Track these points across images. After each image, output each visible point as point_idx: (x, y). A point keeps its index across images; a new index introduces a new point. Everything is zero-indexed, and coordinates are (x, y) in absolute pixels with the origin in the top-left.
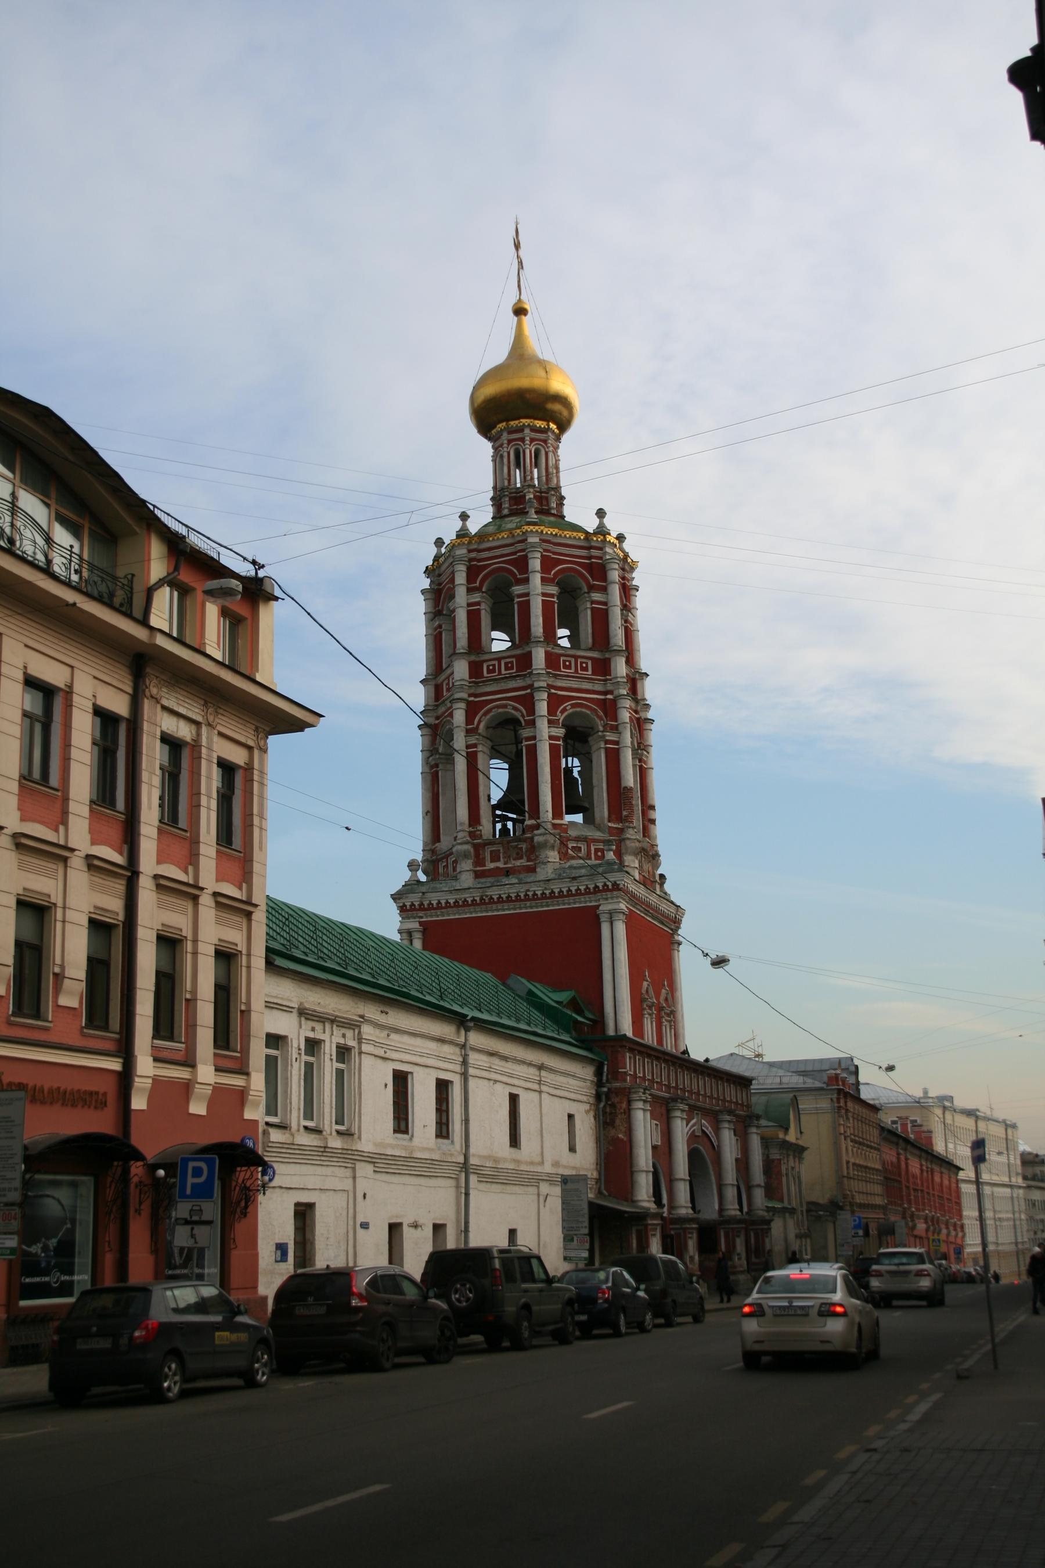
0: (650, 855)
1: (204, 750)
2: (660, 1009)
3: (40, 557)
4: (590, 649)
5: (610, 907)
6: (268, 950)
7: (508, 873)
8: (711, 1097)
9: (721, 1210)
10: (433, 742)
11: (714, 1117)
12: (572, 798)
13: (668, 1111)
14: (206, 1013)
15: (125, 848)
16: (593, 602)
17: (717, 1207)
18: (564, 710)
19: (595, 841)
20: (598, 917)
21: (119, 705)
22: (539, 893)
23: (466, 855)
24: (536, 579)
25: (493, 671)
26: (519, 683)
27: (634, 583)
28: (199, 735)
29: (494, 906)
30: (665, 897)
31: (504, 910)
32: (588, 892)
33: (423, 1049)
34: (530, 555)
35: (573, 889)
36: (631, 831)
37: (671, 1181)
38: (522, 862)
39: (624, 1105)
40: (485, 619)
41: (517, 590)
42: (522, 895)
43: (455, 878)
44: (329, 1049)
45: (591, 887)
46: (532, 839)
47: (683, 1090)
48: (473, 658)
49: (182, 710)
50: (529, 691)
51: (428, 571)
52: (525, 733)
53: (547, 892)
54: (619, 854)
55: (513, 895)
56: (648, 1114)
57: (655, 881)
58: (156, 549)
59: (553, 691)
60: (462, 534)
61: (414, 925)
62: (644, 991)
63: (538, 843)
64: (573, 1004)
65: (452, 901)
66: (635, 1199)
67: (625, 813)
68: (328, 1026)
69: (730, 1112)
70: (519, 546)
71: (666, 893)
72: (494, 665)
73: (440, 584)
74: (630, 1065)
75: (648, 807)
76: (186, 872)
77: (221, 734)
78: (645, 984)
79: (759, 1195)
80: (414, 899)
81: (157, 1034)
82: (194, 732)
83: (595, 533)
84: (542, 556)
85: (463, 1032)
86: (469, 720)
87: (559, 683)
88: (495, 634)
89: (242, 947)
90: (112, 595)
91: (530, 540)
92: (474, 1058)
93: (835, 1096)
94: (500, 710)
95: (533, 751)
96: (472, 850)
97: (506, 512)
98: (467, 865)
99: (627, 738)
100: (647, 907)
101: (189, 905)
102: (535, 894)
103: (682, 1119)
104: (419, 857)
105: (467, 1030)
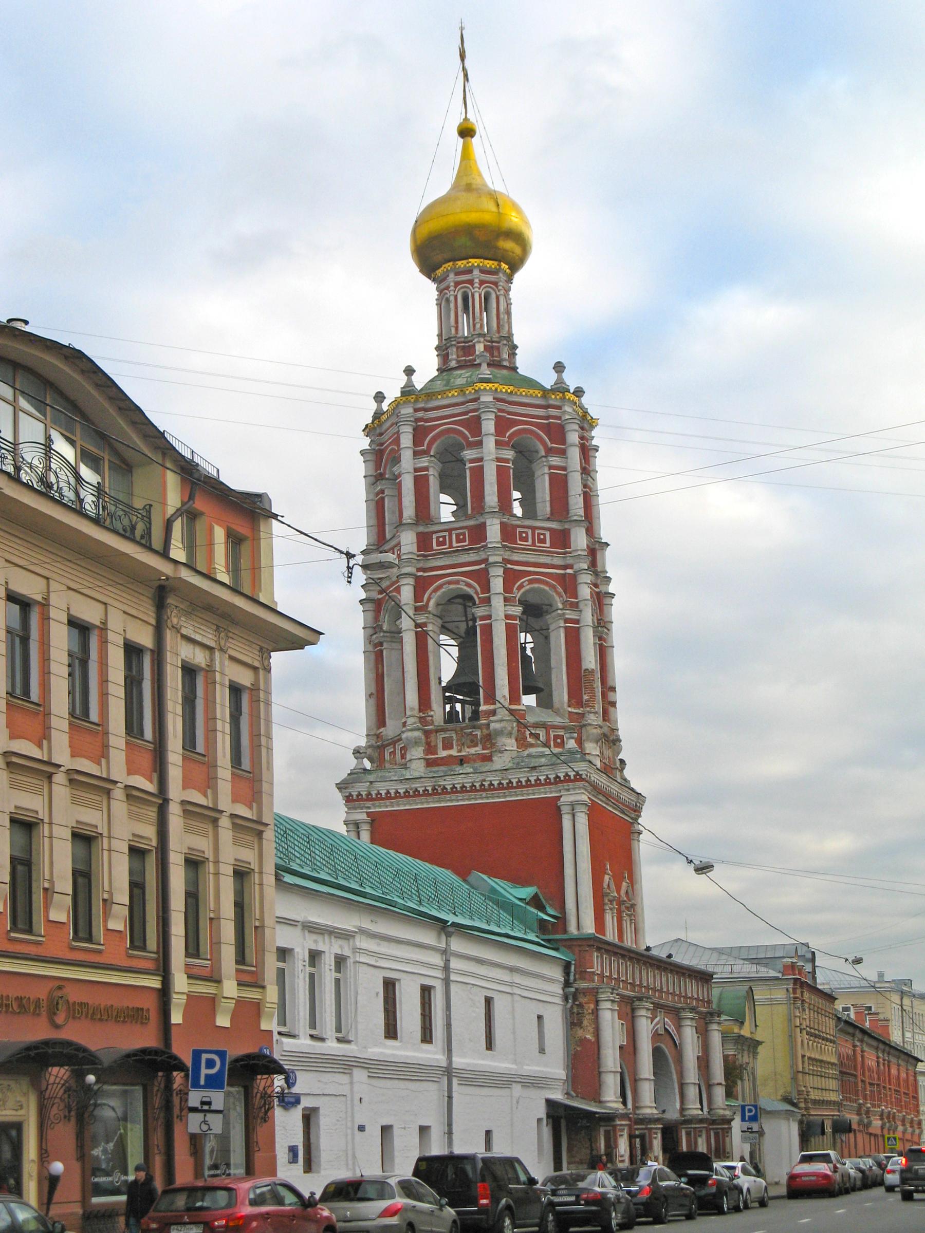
0: (611, 740)
1: (218, 676)
2: (620, 903)
3: (69, 495)
4: (548, 519)
5: (572, 798)
6: (278, 867)
7: (462, 761)
8: (673, 994)
9: (682, 1109)
10: (376, 618)
11: (675, 1013)
12: (530, 679)
13: (633, 1010)
14: (228, 931)
15: (155, 776)
16: (551, 467)
17: (678, 1106)
18: (521, 586)
19: (555, 727)
20: (558, 809)
21: (145, 638)
22: (496, 783)
23: (416, 743)
24: (490, 443)
25: (444, 543)
26: (472, 557)
27: (594, 442)
28: (212, 660)
29: (448, 797)
30: (625, 784)
31: (458, 801)
32: (548, 782)
33: (411, 956)
34: (483, 417)
35: (532, 779)
36: (592, 716)
37: (636, 1081)
38: (478, 750)
39: (592, 1006)
40: (434, 483)
42: (477, 785)
43: (405, 767)
44: (328, 962)
45: (552, 777)
46: (488, 725)
47: (647, 988)
48: (421, 529)
49: (198, 638)
50: (483, 566)
51: (368, 430)
52: (480, 612)
53: (505, 782)
54: (580, 742)
55: (468, 785)
56: (616, 1014)
57: (613, 767)
58: (172, 480)
59: (509, 566)
60: (408, 391)
61: (361, 816)
62: (605, 885)
63: (495, 730)
64: (535, 901)
65: (402, 791)
66: (603, 1099)
67: (585, 697)
68: (326, 937)
69: (693, 1010)
70: (471, 406)
71: (625, 780)
72: (444, 537)
73: (382, 444)
74: (597, 963)
75: (609, 689)
76: (205, 795)
77: (232, 658)
78: (607, 877)
79: (719, 1093)
80: (361, 788)
81: (188, 955)
82: (208, 658)
83: (553, 390)
84: (496, 417)
85: (444, 937)
86: (418, 596)
87: (516, 557)
88: (444, 498)
89: (254, 866)
90: (133, 528)
91: (483, 399)
92: (455, 964)
93: (791, 986)
94: (452, 586)
95: (488, 631)
96: (423, 737)
97: (453, 364)
98: (417, 752)
99: (588, 616)
100: (607, 796)
101: (210, 828)
102: (491, 784)
103: (647, 1017)
104: (363, 742)
105: (449, 935)
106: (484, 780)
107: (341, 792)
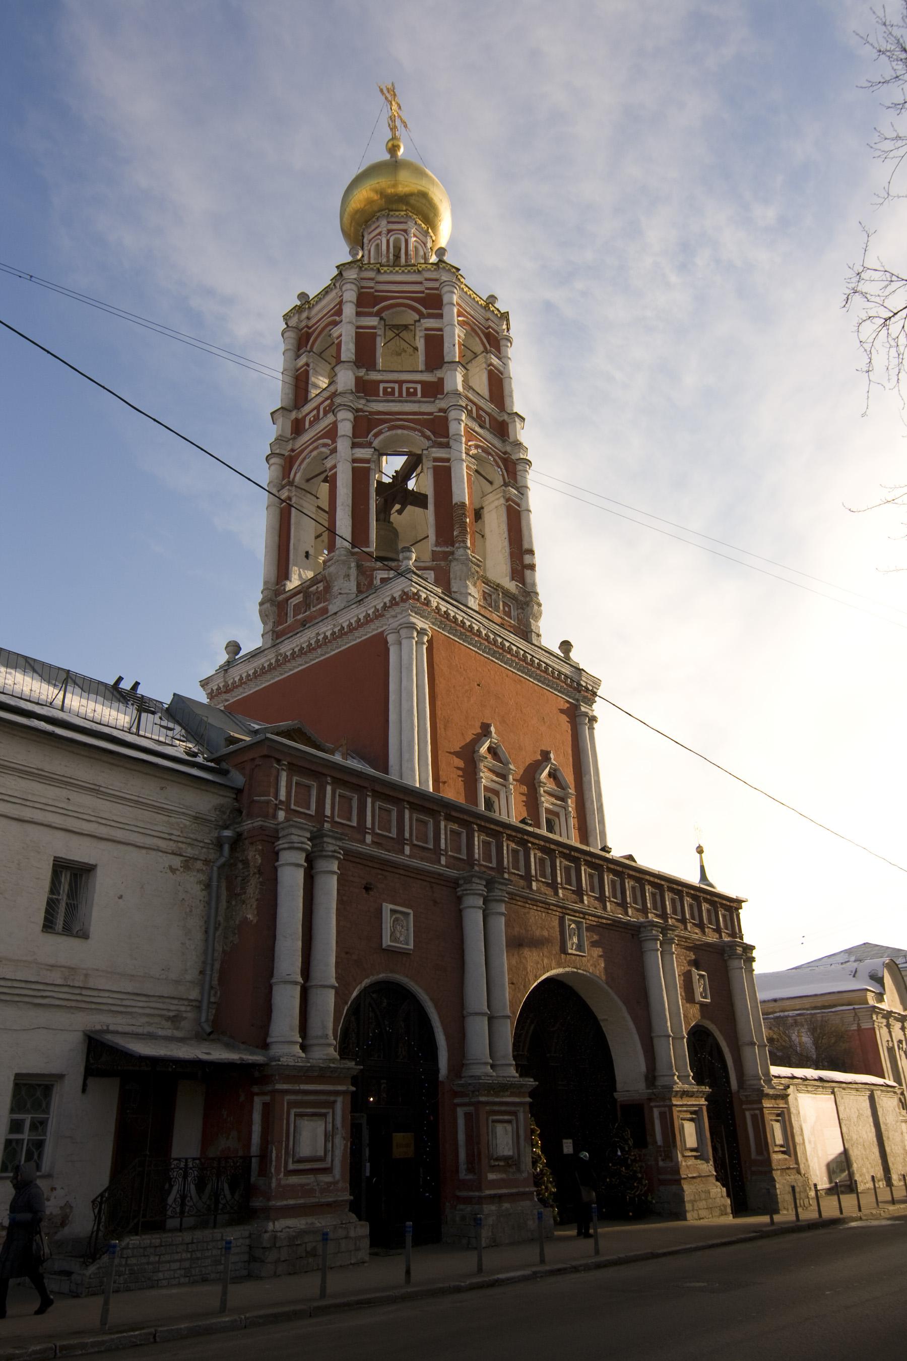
5: (395, 625)
13: (459, 899)
17: (643, 1068)
18: (380, 433)
22: (328, 634)
41: (335, 332)
42: (313, 642)
48: (294, 415)
53: (336, 630)
65: (251, 672)
67: (455, 533)
94: (315, 453)
102: (325, 637)
106: (318, 634)
107: (204, 689)
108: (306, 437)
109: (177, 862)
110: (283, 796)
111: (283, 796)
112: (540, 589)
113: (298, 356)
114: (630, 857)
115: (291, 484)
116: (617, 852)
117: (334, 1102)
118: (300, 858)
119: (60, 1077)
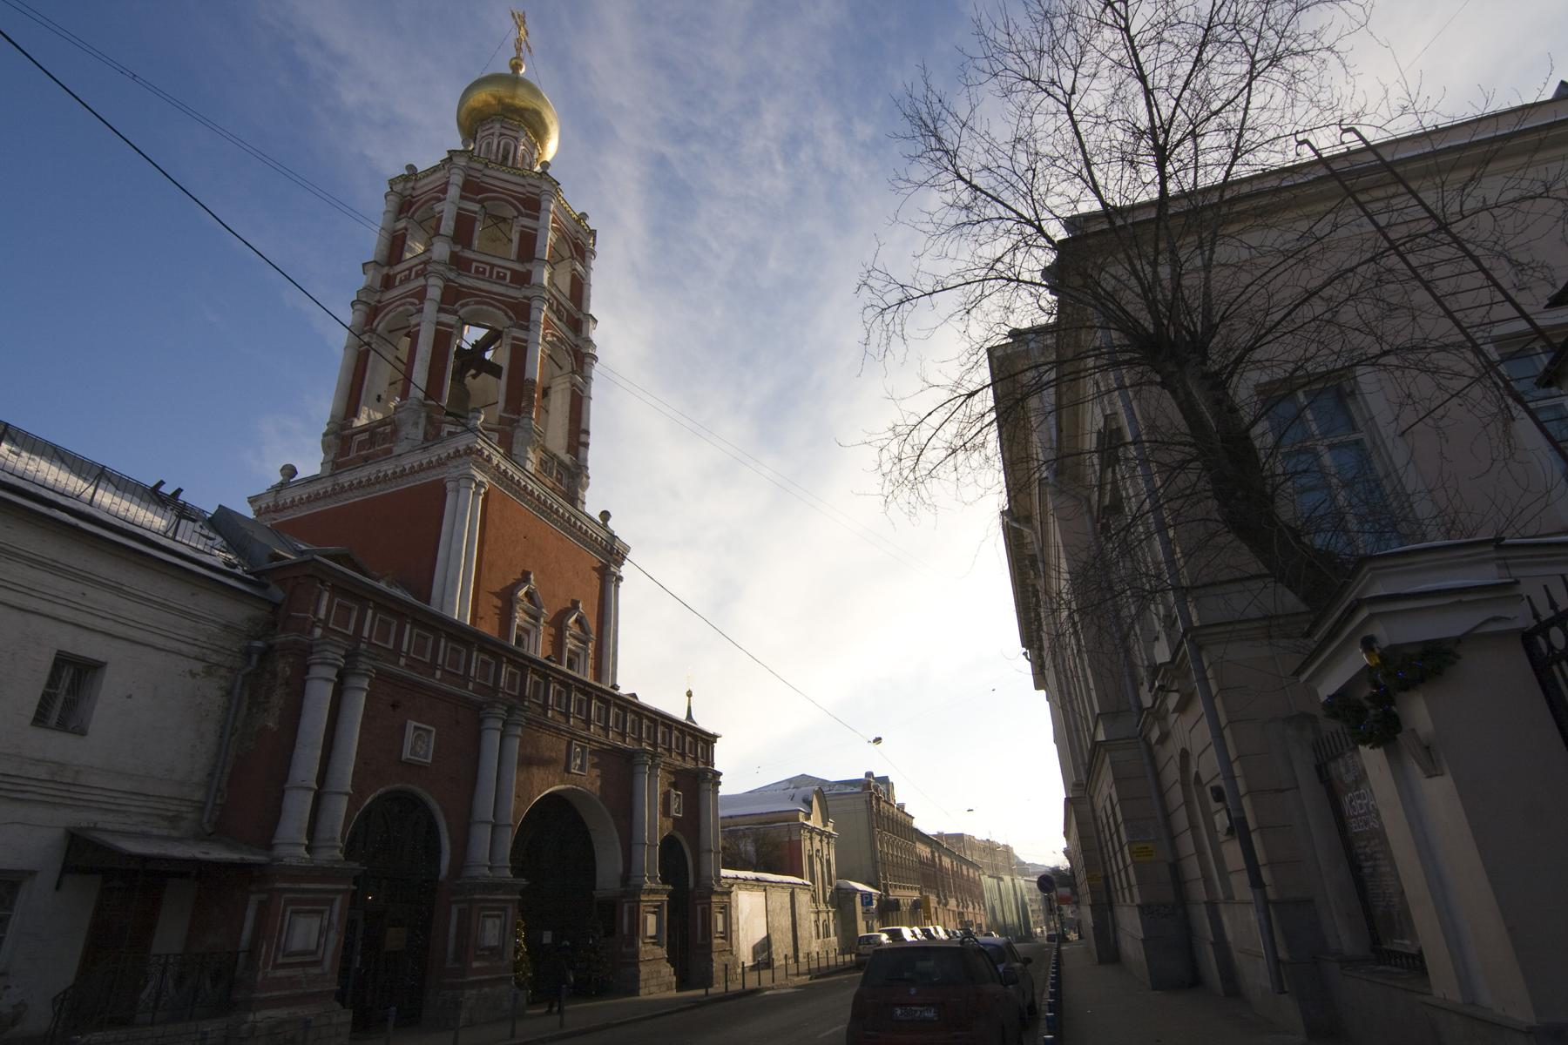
13: (481, 721)
17: (621, 870)
18: (467, 304)
20: (445, 488)
41: (438, 207)
48: (385, 270)
102: (386, 475)
108: (394, 293)
109: (199, 667)
110: (322, 614)
111: (322, 614)
112: (589, 464)
113: (398, 220)
114: (634, 695)
115: (373, 331)
116: (624, 690)
117: (334, 900)
118: (332, 673)
119: (32, 873)
